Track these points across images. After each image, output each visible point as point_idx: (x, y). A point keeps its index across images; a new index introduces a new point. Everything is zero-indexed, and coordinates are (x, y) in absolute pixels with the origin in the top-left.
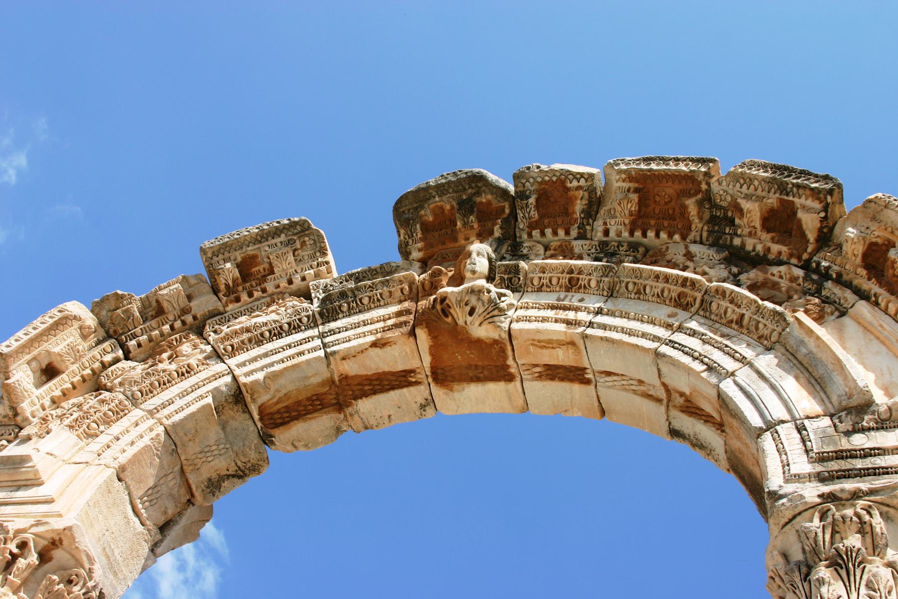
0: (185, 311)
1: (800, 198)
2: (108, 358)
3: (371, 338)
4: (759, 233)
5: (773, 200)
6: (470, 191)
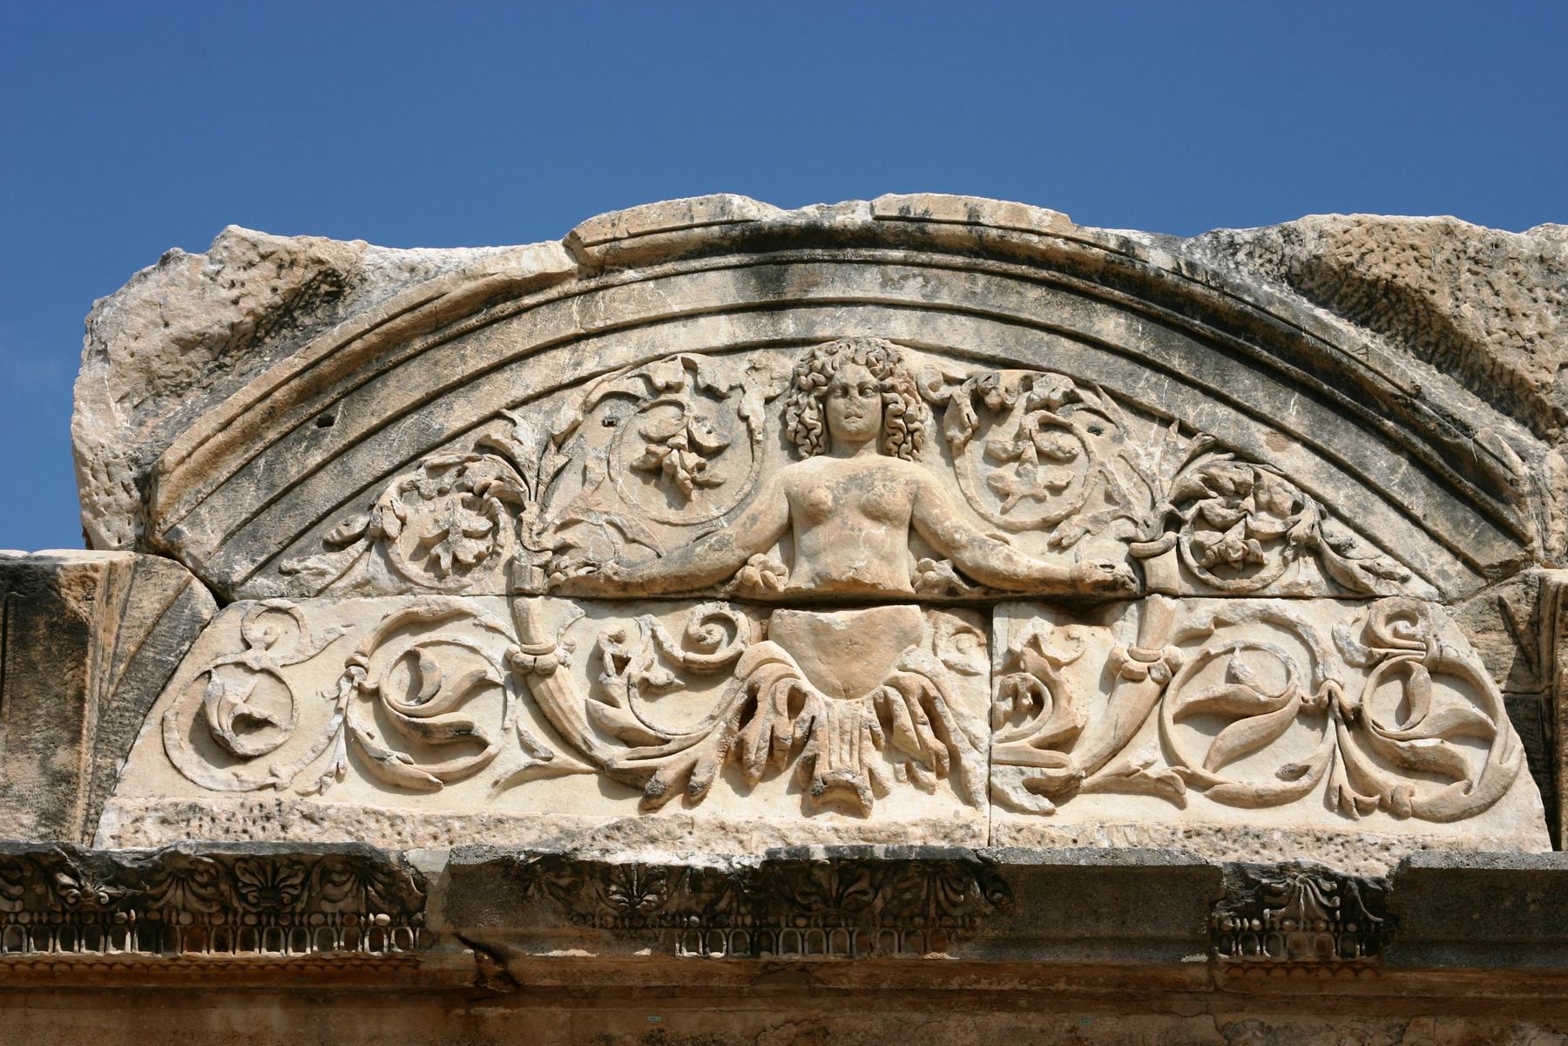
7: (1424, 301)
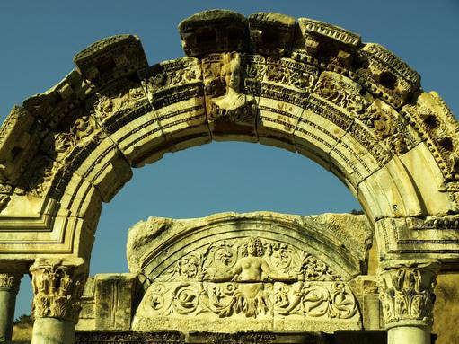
0: (73, 97)
2: (42, 135)
3: (185, 125)
5: (386, 70)
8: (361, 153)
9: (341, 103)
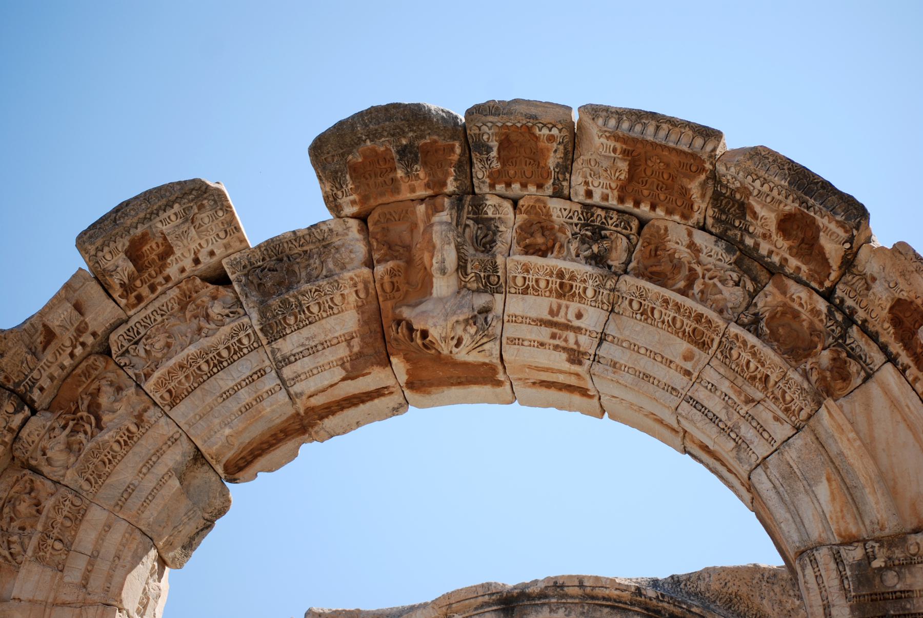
0: (80, 331)
1: (822, 217)
4: (774, 237)
5: (790, 206)
6: (411, 134)
7: (749, 598)
8: (749, 401)
9: (697, 287)
